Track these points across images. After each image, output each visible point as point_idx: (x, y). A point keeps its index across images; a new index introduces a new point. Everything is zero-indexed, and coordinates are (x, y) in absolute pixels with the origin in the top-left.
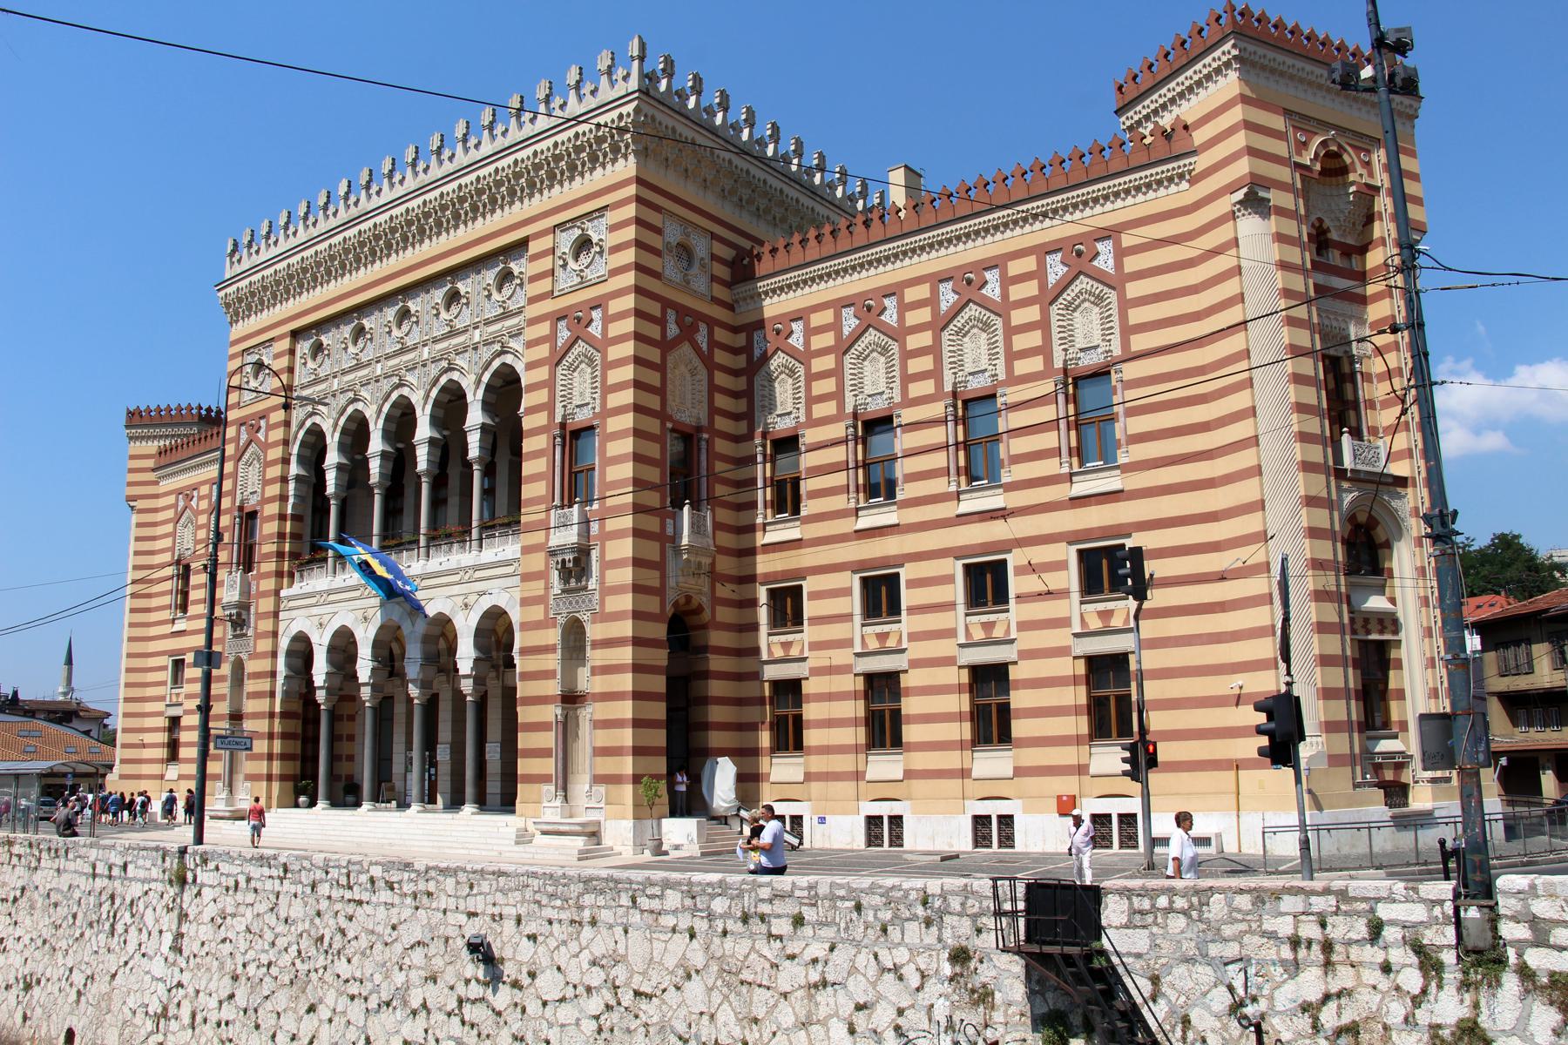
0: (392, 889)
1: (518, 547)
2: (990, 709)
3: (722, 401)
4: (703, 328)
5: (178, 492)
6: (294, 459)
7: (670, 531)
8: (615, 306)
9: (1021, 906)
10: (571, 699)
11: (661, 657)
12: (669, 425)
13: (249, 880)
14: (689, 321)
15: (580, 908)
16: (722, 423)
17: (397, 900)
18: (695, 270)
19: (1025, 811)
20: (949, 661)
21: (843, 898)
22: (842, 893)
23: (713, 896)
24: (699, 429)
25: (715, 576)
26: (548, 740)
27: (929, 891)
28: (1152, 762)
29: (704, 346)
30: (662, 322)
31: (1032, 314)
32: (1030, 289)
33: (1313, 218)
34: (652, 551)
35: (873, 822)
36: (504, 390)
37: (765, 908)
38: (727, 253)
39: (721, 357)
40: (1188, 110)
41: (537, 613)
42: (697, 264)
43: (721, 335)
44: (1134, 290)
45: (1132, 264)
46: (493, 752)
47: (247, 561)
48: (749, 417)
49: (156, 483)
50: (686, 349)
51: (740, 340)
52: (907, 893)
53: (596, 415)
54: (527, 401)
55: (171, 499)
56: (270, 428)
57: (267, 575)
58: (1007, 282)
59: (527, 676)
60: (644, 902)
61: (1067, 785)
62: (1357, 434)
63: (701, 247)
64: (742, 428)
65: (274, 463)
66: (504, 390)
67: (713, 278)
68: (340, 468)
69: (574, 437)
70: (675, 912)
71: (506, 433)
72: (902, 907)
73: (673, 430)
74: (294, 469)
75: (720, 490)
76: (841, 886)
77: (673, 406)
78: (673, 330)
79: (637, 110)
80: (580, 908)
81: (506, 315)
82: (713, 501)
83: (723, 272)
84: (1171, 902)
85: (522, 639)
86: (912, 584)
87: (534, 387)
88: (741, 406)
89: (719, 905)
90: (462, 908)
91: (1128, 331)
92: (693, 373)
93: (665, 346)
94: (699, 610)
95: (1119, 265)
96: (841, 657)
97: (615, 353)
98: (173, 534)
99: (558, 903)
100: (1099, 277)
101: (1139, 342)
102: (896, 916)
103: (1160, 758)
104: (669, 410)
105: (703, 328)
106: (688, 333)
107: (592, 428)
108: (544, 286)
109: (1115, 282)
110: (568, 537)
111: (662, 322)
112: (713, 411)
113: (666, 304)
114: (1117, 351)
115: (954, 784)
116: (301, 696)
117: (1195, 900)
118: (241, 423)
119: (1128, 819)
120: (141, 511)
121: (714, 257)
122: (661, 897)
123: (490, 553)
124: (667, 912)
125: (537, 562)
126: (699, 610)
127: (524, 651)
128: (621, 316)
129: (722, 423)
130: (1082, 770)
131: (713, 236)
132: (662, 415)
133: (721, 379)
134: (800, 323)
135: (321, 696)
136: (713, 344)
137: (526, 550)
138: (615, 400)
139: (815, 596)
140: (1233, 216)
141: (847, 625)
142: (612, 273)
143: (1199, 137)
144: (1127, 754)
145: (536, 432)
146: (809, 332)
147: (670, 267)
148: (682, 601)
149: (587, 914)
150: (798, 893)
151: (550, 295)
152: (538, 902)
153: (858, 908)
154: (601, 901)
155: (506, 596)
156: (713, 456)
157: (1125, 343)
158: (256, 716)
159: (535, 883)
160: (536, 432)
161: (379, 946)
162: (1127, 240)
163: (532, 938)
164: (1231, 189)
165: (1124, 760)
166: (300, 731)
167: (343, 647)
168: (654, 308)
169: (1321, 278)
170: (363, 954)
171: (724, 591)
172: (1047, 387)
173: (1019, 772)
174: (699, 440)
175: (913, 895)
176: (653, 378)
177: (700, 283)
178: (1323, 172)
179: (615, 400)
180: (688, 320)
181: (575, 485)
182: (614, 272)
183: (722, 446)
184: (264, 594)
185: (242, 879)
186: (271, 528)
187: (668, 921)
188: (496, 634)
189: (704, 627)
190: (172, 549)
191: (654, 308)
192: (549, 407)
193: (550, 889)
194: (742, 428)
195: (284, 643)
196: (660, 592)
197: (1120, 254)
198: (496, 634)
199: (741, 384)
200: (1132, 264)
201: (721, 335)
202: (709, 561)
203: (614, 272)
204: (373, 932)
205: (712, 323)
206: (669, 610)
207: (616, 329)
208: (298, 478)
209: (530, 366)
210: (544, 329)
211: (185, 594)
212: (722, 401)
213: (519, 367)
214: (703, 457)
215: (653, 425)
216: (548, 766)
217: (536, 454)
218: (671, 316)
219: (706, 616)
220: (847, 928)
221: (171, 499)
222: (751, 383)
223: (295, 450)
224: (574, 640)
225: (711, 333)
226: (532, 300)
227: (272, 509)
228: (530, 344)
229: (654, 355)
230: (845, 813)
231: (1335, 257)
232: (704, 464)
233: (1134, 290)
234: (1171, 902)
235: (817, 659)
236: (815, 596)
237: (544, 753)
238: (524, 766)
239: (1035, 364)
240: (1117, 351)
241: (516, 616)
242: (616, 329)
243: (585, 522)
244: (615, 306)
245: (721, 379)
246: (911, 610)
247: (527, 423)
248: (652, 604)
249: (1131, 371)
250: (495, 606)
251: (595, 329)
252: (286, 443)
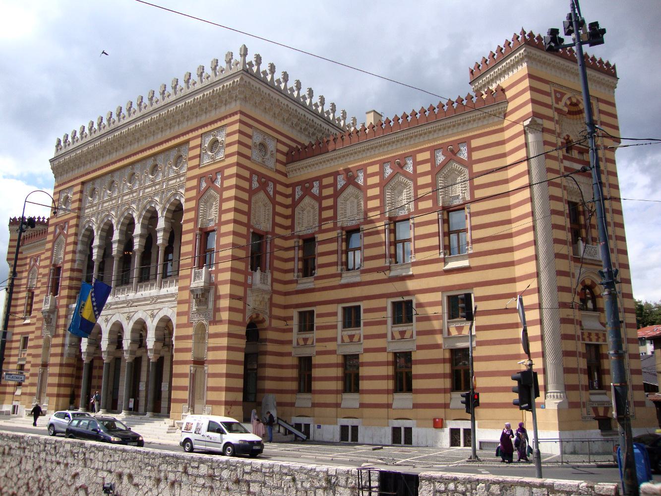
0: (74, 456)
1: (177, 287)
3: (278, 220)
4: (271, 184)
5: (31, 258)
6: (79, 243)
7: (249, 282)
8: (227, 172)
9: (375, 484)
10: (199, 362)
11: (242, 343)
12: (252, 230)
13: (10, 449)
14: (264, 181)
15: (160, 471)
16: (278, 230)
17: (76, 462)
18: (268, 156)
19: (418, 426)
20: (383, 350)
21: (286, 474)
22: (285, 471)
23: (222, 469)
24: (267, 233)
25: (272, 305)
26: (186, 382)
27: (329, 473)
28: (477, 404)
29: (271, 193)
30: (250, 180)
31: (428, 179)
32: (427, 167)
33: (564, 135)
34: (240, 291)
35: (344, 428)
36: (176, 211)
37: (247, 477)
38: (285, 149)
39: (279, 198)
40: (504, 82)
41: (184, 320)
42: (269, 153)
43: (280, 188)
44: (477, 168)
45: (476, 155)
46: (165, 387)
47: (55, 289)
48: (292, 227)
50: (262, 195)
51: (289, 191)
52: (318, 473)
53: (216, 225)
54: (186, 217)
56: (70, 227)
57: (63, 298)
58: (416, 164)
59: (178, 350)
60: (190, 470)
61: (439, 413)
62: (586, 241)
63: (272, 146)
64: (288, 233)
65: (70, 244)
66: (176, 211)
67: (277, 161)
68: (99, 247)
69: (205, 234)
70: (203, 477)
71: (174, 234)
72: (315, 481)
73: (253, 233)
75: (277, 263)
76: (285, 467)
77: (253, 222)
78: (255, 185)
79: (242, 79)
80: (160, 471)
81: (179, 176)
82: (273, 269)
83: (283, 158)
84: (456, 487)
85: (176, 331)
86: (366, 311)
87: (189, 210)
88: (288, 222)
89: (225, 474)
90: (105, 468)
91: (473, 188)
92: (265, 206)
93: (251, 192)
94: (263, 321)
95: (470, 156)
96: (330, 346)
97: (226, 194)
99: (149, 468)
100: (461, 162)
101: (479, 194)
102: (312, 486)
103: (481, 401)
104: (252, 224)
105: (271, 184)
106: (263, 186)
107: (214, 231)
108: (195, 162)
109: (469, 164)
110: (200, 283)
111: (250, 180)
112: (275, 224)
113: (253, 172)
114: (468, 198)
115: (383, 411)
116: (76, 356)
117: (469, 486)
118: (56, 225)
119: (467, 431)
121: (278, 151)
122: (198, 468)
123: (164, 291)
124: (200, 476)
125: (186, 295)
126: (263, 321)
127: (177, 338)
128: (230, 176)
129: (278, 230)
131: (278, 141)
132: (248, 225)
133: (279, 209)
134: (317, 182)
135: (84, 357)
136: (276, 192)
137: (180, 289)
138: (225, 217)
139: (321, 315)
141: (334, 331)
142: (226, 159)
143: (509, 94)
144: (464, 399)
145: (188, 232)
146: (322, 187)
147: (255, 155)
148: (254, 316)
149: (162, 474)
150: (264, 470)
152: (140, 467)
153: (294, 480)
154: (169, 468)
155: (169, 311)
156: (273, 246)
157: (472, 194)
158: (54, 365)
159: (139, 456)
160: (188, 232)
161: (65, 487)
162: (475, 143)
163: (136, 485)
164: (524, 119)
165: (462, 402)
166: (75, 373)
168: (247, 174)
169: (567, 163)
170: (57, 490)
171: (276, 312)
172: (434, 216)
173: (416, 406)
174: (267, 238)
175: (321, 475)
176: (245, 207)
177: (271, 163)
178: (570, 113)
179: (225, 217)
180: (263, 180)
181: (204, 256)
182: (227, 156)
183: (278, 241)
184: (62, 306)
185: (7, 448)
186: (67, 274)
187: (201, 481)
189: (265, 329)
191: (247, 174)
192: (195, 220)
193: (146, 461)
194: (288, 233)
196: (243, 311)
197: (471, 150)
198: (165, 328)
199: (288, 212)
200: (476, 155)
201: (280, 188)
202: (269, 297)
203: (227, 156)
204: (63, 479)
205: (275, 182)
206: (248, 320)
207: (227, 183)
208: (80, 252)
209: (187, 200)
210: (194, 183)
211: (31, 305)
212: (278, 220)
213: (183, 200)
214: (268, 247)
215: (243, 230)
216: (185, 395)
217: (188, 243)
218: (255, 178)
219: (267, 324)
220: (287, 491)
222: (293, 212)
224: (201, 334)
225: (275, 187)
226: (189, 169)
227: (67, 266)
228: (187, 190)
229: (245, 196)
230: (330, 424)
231: (575, 154)
232: (268, 250)
233: (477, 168)
234: (456, 487)
235: (320, 347)
236: (321, 315)
237: (183, 388)
238: (175, 395)
239: (428, 204)
240: (468, 198)
241: (174, 321)
242: (227, 183)
243: (209, 274)
244: (227, 172)
245: (279, 209)
246: (366, 324)
247: (185, 227)
248: (239, 317)
249: (475, 207)
250: (165, 316)
251: (218, 184)
252: (76, 234)
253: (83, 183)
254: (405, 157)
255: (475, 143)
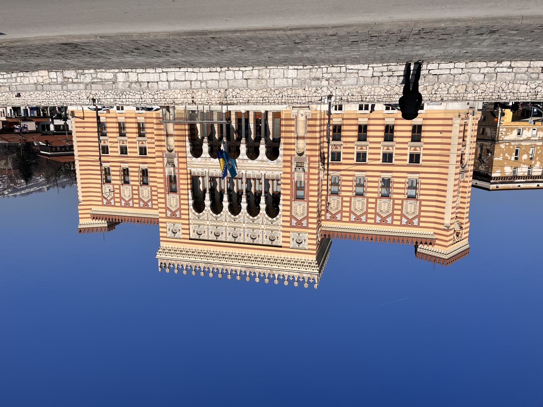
2: (122, 129)
5: (418, 226)
40: (90, 221)
45: (100, 199)
49: (435, 233)
55: (421, 224)
61: (108, 115)
74: (281, 207)
96: (149, 140)
98: (420, 211)
120: (443, 224)
130: (106, 117)
140: (83, 201)
143: (89, 216)
151: (183, 224)
162: (101, 203)
167: (253, 153)
188: (197, 152)
190: (421, 205)
195: (279, 158)
200: (100, 199)
210: (183, 217)
221: (421, 224)
223: (280, 213)
241: (190, 155)
253: (281, 247)
254: (125, 207)
255: (101, 203)
